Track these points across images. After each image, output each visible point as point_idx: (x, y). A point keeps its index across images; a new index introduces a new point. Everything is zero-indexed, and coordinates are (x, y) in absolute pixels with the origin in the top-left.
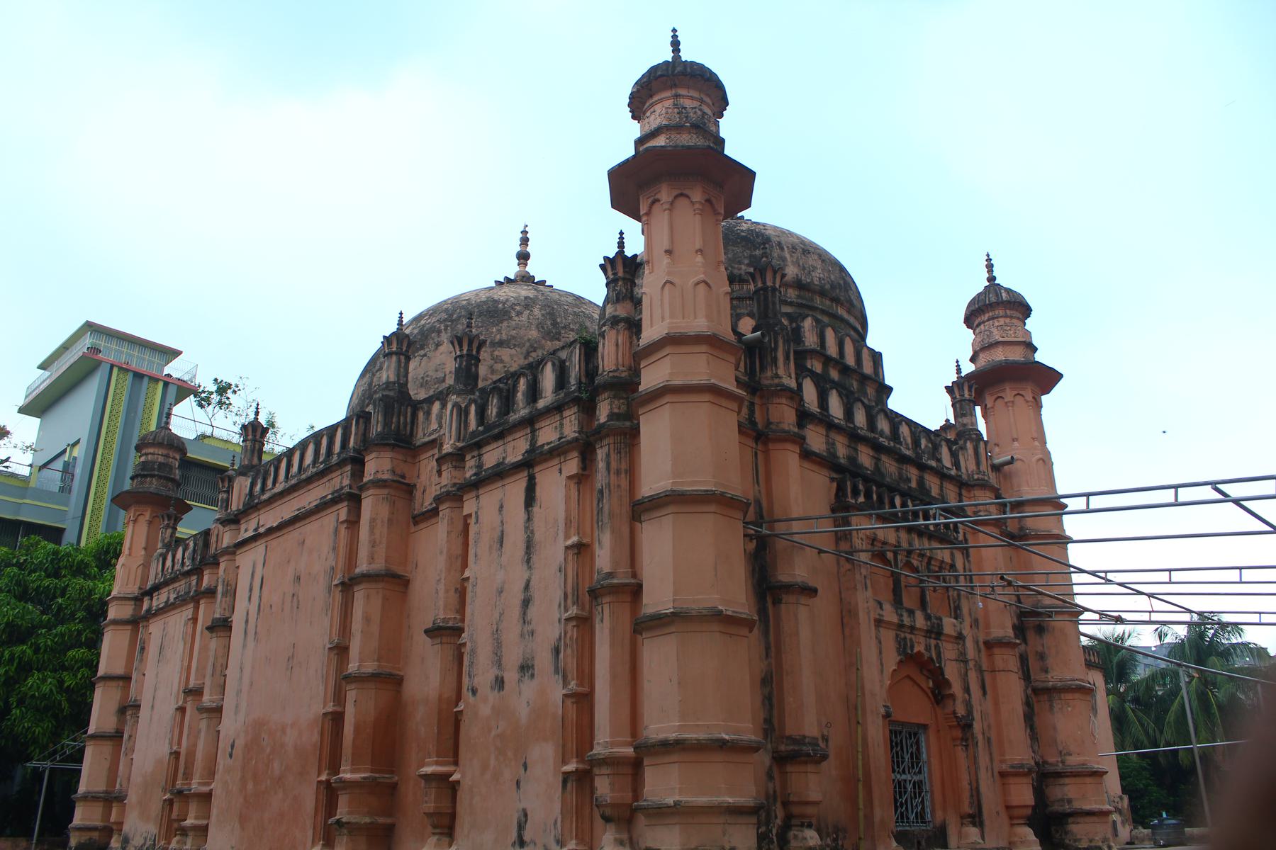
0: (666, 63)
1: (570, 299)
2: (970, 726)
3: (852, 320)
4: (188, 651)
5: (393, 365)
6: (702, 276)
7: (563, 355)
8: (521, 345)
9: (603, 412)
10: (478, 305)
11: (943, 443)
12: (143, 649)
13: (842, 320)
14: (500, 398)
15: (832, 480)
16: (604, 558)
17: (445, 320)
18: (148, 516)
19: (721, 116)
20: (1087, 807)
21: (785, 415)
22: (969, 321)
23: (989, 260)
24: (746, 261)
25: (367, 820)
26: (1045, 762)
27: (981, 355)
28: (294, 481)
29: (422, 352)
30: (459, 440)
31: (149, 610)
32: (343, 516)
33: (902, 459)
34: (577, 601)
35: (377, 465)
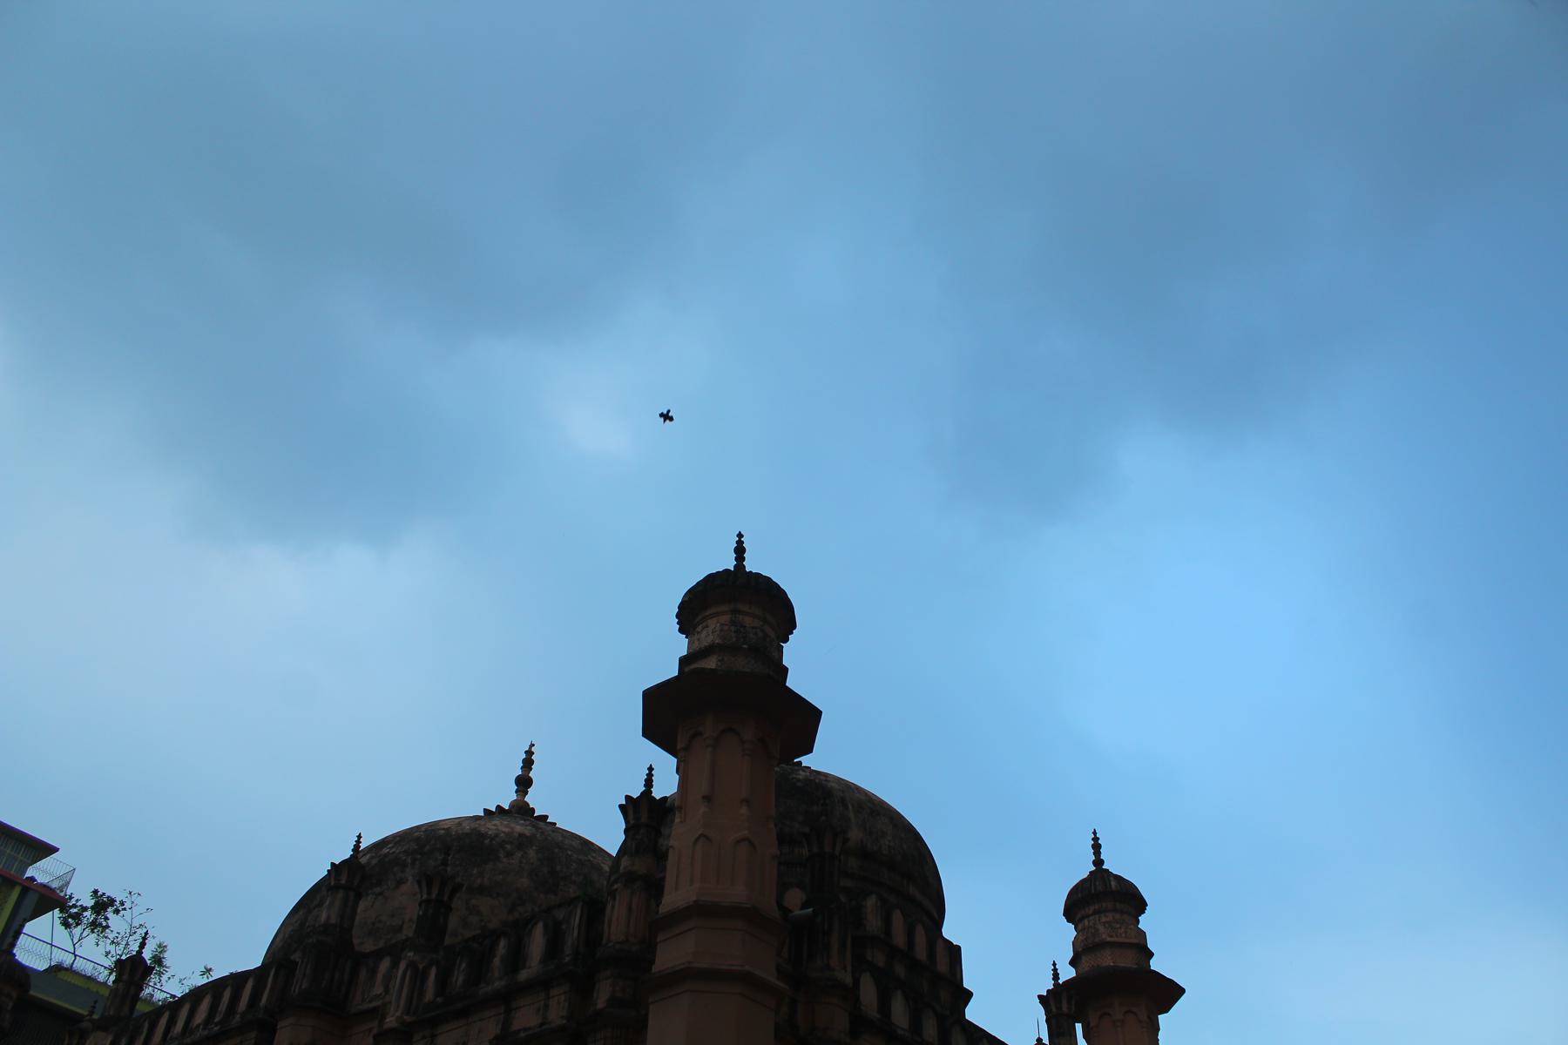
0: (727, 571)
1: (575, 843)
7: (560, 914)
9: (603, 995)
19: (786, 640)
22: (1071, 912)
23: (1096, 839)
27: (1084, 959)
29: (378, 890)
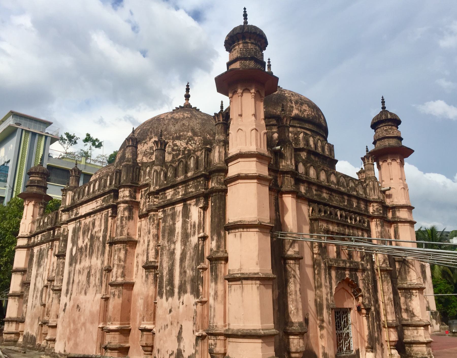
0: (241, 26)
6: (254, 127)
7: (199, 153)
8: (185, 139)
18: (33, 203)
19: (265, 49)
23: (383, 99)
27: (378, 142)
29: (144, 141)
35: (124, 193)
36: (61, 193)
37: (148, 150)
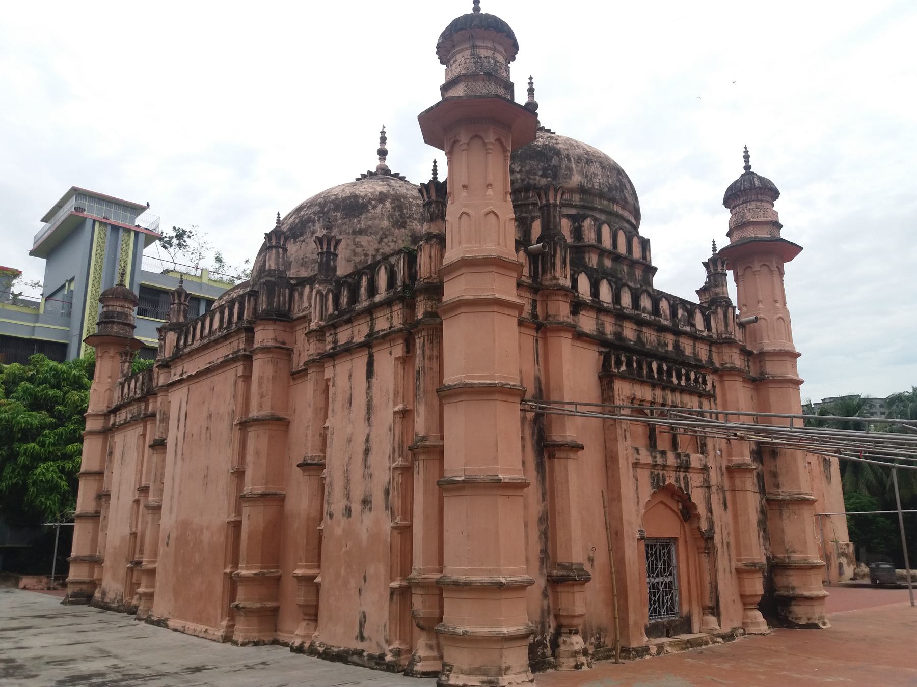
2: (711, 538)
3: (626, 214)
4: (140, 458)
5: (273, 257)
7: (393, 260)
8: (376, 233)
10: (344, 199)
11: (698, 311)
12: (111, 453)
13: (617, 215)
14: (349, 291)
15: (600, 353)
16: (420, 425)
17: (319, 212)
19: (513, 59)
20: (807, 594)
21: (562, 309)
23: (746, 152)
24: (540, 173)
25: (258, 605)
26: (774, 557)
28: (206, 341)
29: (301, 238)
30: (321, 319)
31: (114, 425)
32: (240, 373)
33: (661, 329)
34: (401, 455)
35: (264, 335)
36: (158, 335)
37: (308, 255)
